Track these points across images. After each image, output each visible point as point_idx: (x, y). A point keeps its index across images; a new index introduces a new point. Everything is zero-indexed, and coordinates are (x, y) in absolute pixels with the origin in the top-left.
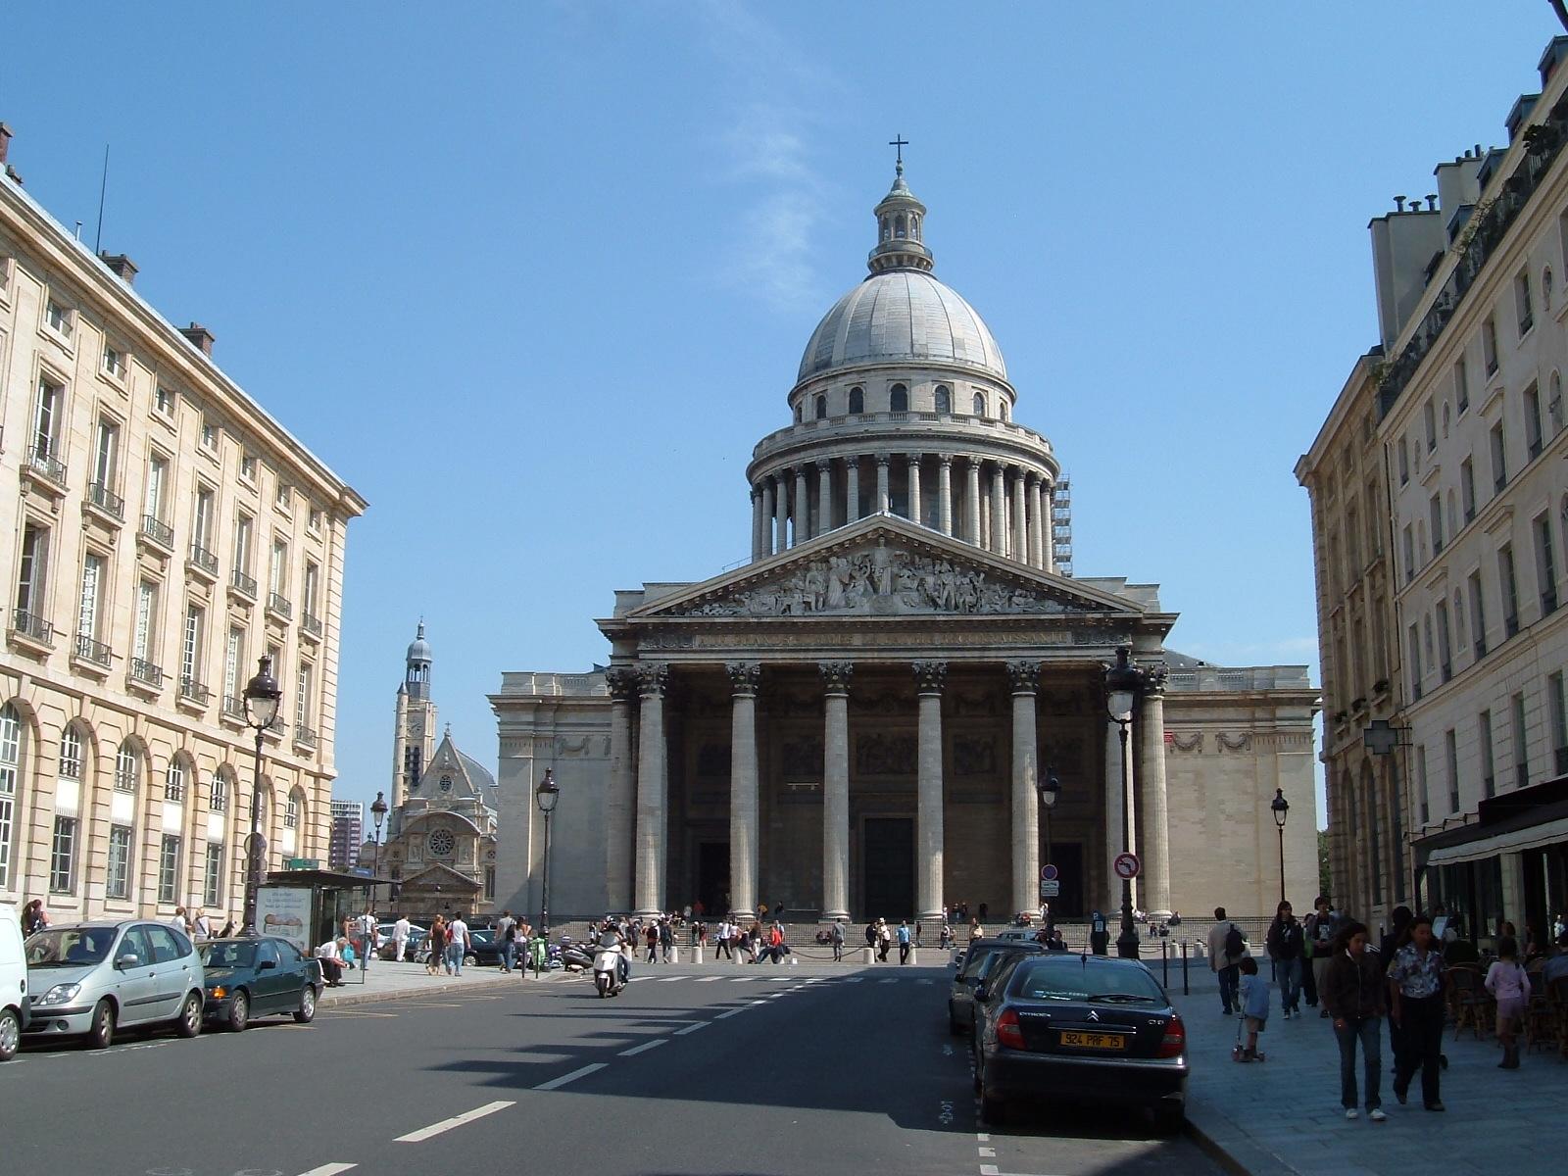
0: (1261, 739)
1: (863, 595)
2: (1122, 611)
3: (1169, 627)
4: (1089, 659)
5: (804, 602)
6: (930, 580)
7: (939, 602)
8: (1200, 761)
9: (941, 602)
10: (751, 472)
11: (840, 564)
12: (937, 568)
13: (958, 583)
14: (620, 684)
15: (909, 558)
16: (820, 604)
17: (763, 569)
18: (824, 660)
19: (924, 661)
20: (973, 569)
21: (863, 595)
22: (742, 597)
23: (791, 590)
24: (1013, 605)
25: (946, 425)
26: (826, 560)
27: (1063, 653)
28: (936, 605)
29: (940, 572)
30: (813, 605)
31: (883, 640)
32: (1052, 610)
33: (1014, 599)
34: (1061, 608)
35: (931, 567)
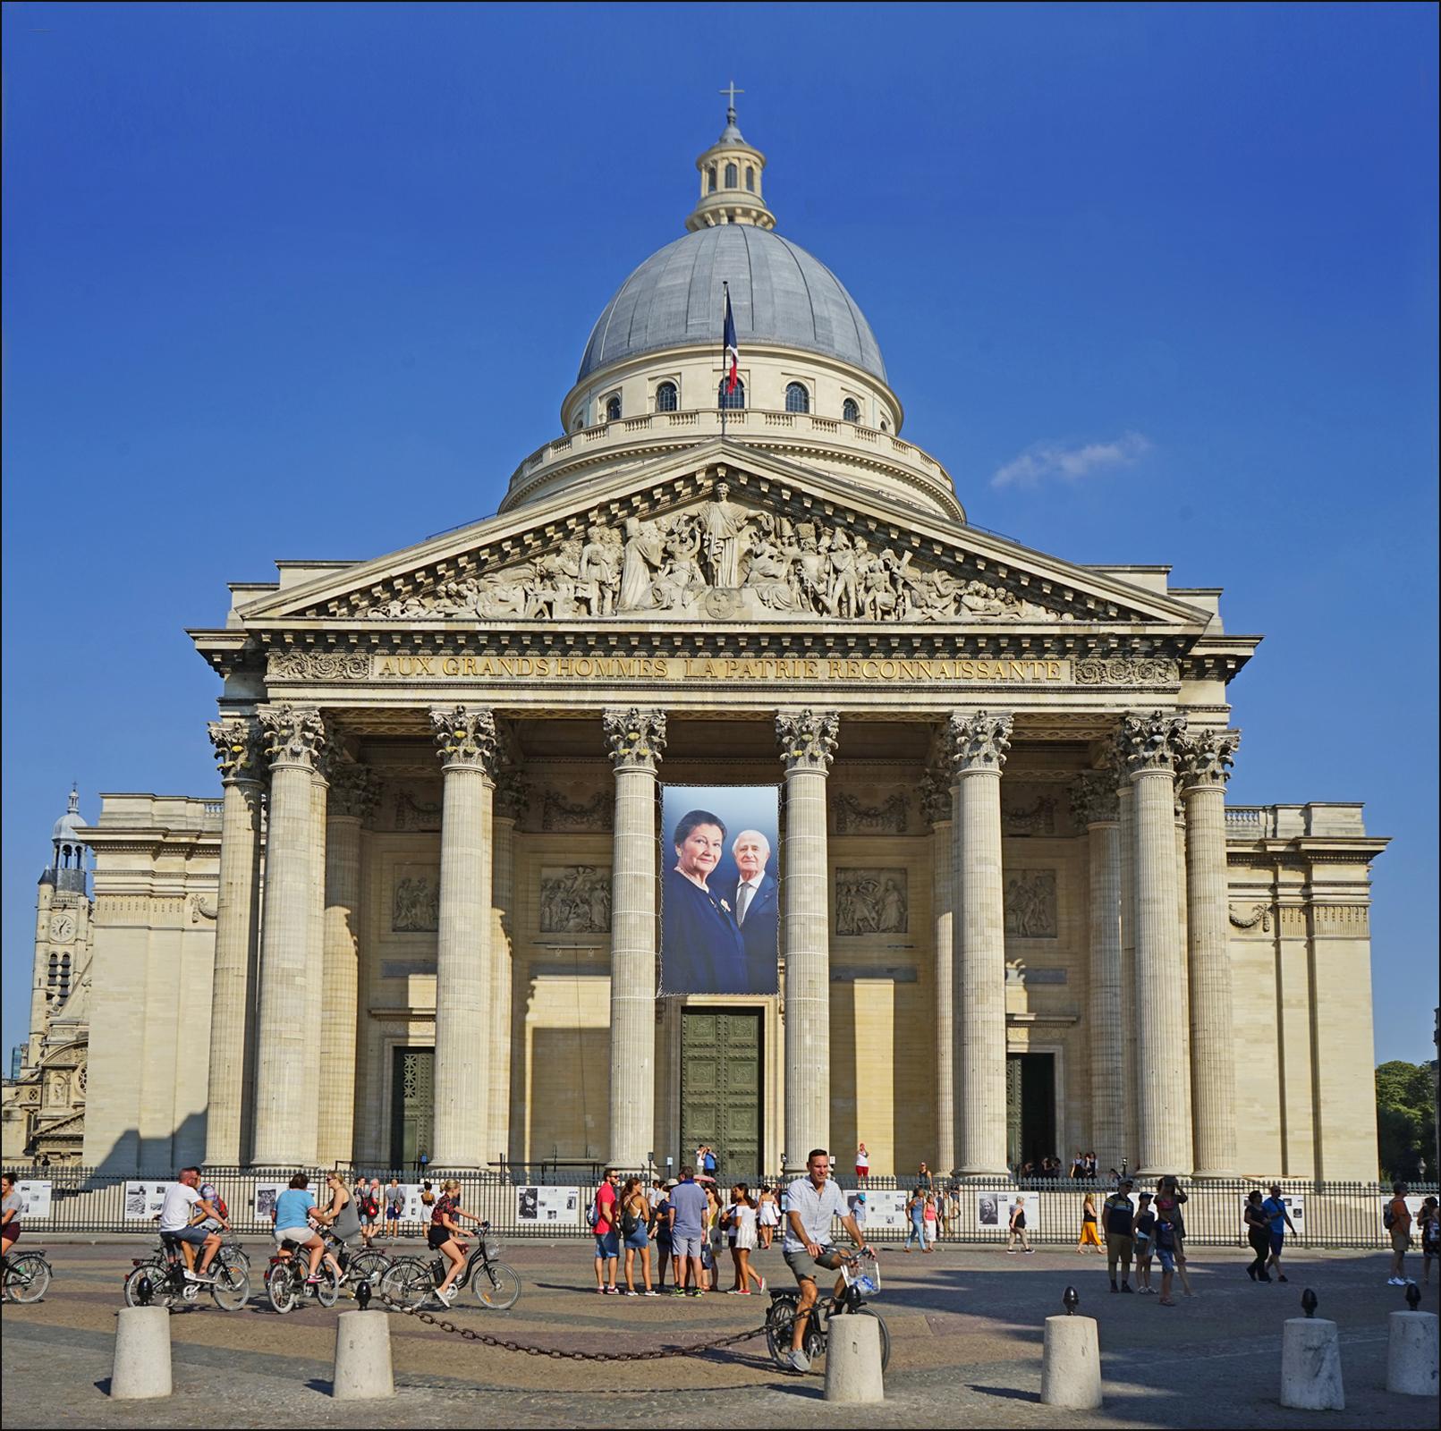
5: (577, 599)
6: (813, 564)
9: (831, 603)
11: (649, 534)
12: (826, 541)
14: (236, 749)
15: (772, 523)
16: (608, 603)
18: (614, 707)
19: (800, 709)
20: (890, 543)
22: (462, 587)
24: (965, 611)
29: (830, 549)
31: (721, 668)
33: (967, 600)
34: (1052, 617)
35: (813, 540)
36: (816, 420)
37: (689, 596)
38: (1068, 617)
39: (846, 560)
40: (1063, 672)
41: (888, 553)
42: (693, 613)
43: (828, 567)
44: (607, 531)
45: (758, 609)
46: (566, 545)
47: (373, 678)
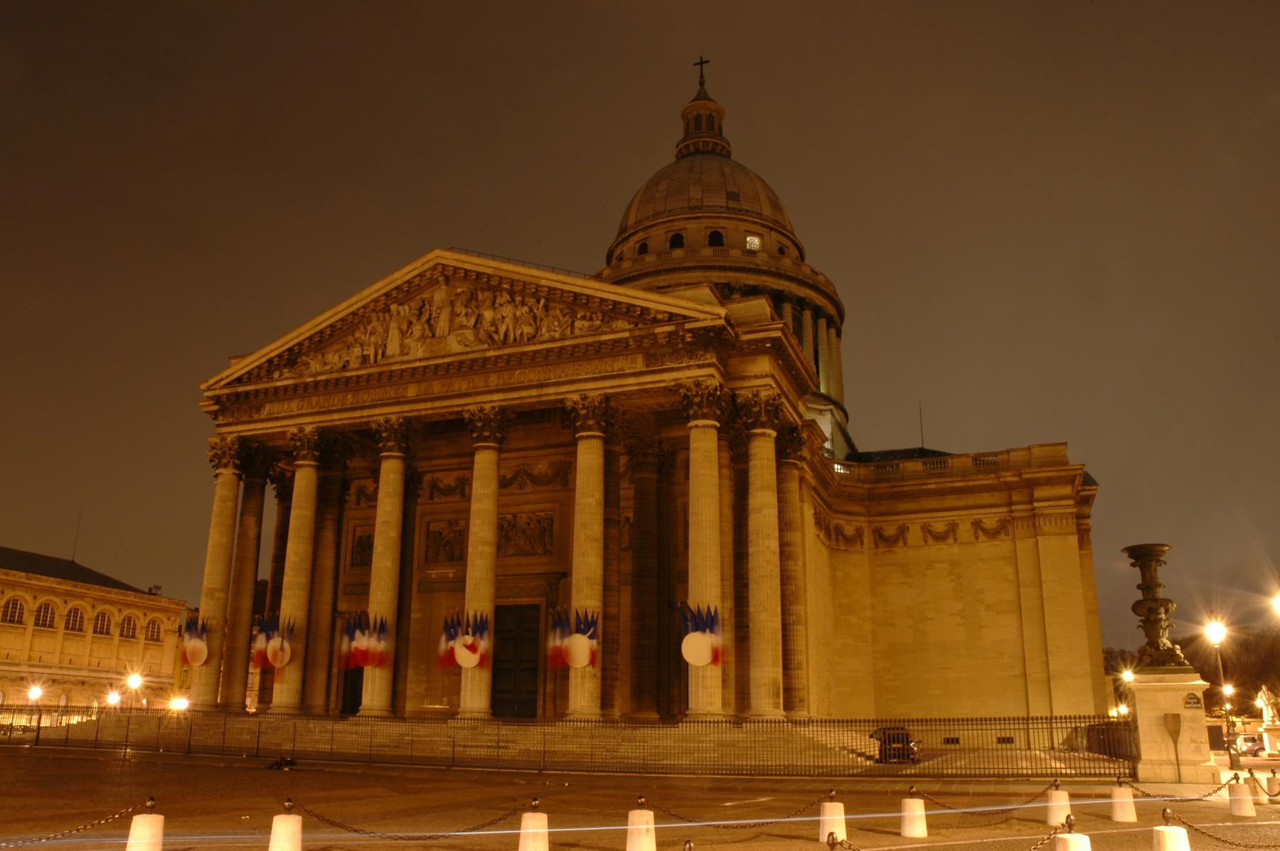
0: (1020, 524)
1: (418, 340)
2: (698, 320)
4: (663, 385)
6: (488, 315)
7: (496, 337)
8: (956, 549)
13: (518, 314)
16: (379, 357)
17: (324, 325)
18: (377, 415)
21: (418, 340)
24: (577, 332)
26: (387, 310)
27: (632, 380)
30: (372, 357)
31: (437, 387)
32: (622, 330)
33: (578, 324)
37: (419, 344)
39: (507, 311)
42: (420, 354)
44: (381, 315)
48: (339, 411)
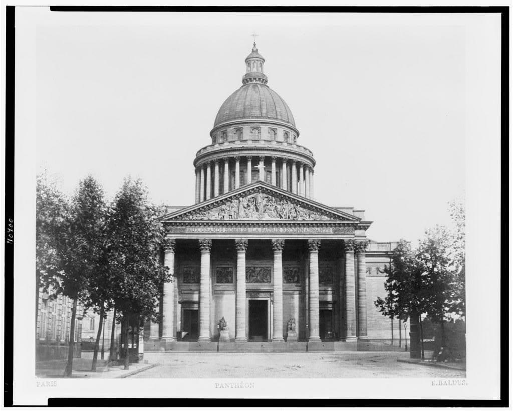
3: (368, 227)
5: (230, 215)
6: (279, 207)
9: (283, 216)
10: (195, 163)
11: (244, 201)
12: (282, 202)
20: (295, 203)
22: (205, 213)
23: (224, 210)
25: (274, 145)
28: (281, 217)
34: (329, 219)
36: (277, 142)
38: (332, 219)
40: (331, 230)
41: (295, 205)
43: (282, 208)
44: (235, 200)
45: (266, 218)
46: (227, 203)
47: (186, 233)
48: (220, 234)
